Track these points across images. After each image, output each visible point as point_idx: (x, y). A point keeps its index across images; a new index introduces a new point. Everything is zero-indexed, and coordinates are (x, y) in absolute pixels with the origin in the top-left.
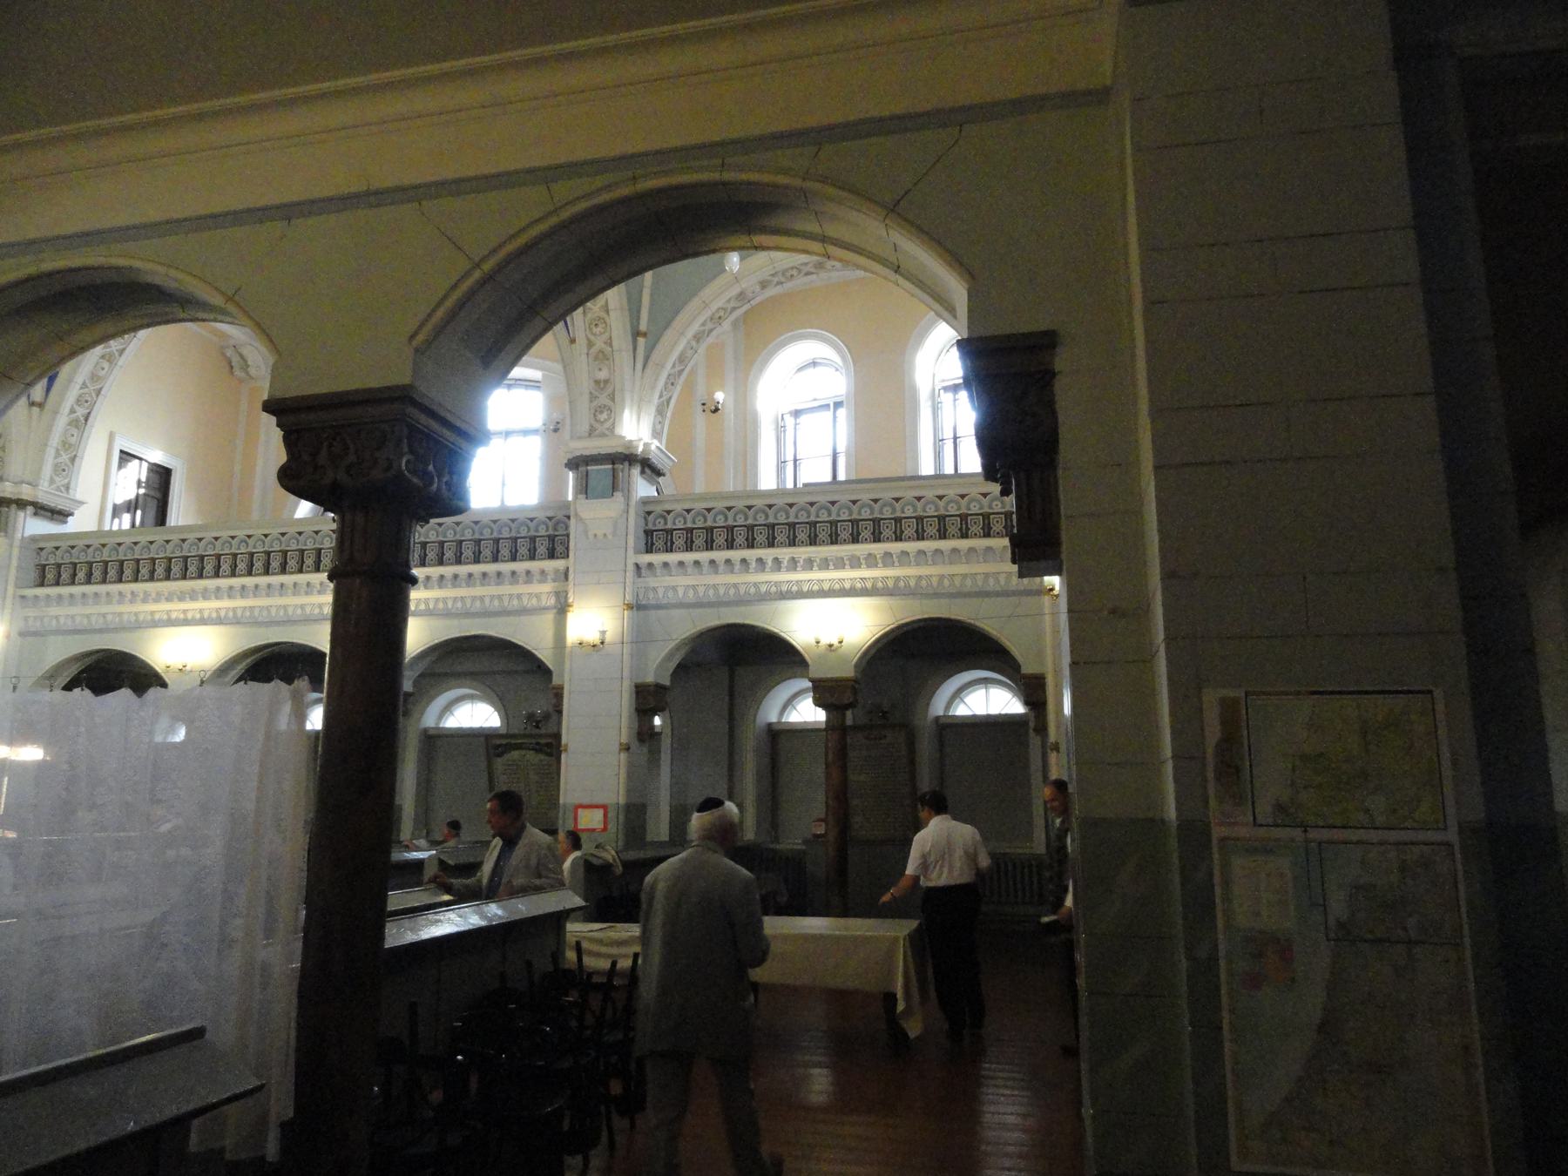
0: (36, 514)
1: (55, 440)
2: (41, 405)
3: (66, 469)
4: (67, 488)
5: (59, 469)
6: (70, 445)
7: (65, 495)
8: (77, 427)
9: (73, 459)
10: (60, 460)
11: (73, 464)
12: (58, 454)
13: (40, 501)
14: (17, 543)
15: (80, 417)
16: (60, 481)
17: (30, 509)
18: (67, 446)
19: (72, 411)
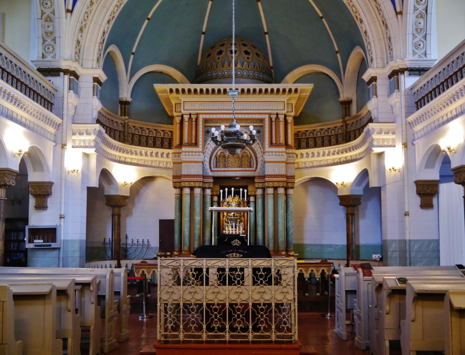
0: (410, 75)
1: (410, 29)
2: (401, 13)
3: (421, 43)
4: (425, 54)
5: (417, 46)
6: (421, 30)
7: (425, 58)
8: (421, 17)
9: (425, 37)
10: (417, 39)
11: (426, 40)
12: (414, 37)
13: (409, 67)
14: (403, 94)
15: (423, 11)
16: (419, 52)
17: (406, 73)
18: (419, 31)
19: (415, 9)
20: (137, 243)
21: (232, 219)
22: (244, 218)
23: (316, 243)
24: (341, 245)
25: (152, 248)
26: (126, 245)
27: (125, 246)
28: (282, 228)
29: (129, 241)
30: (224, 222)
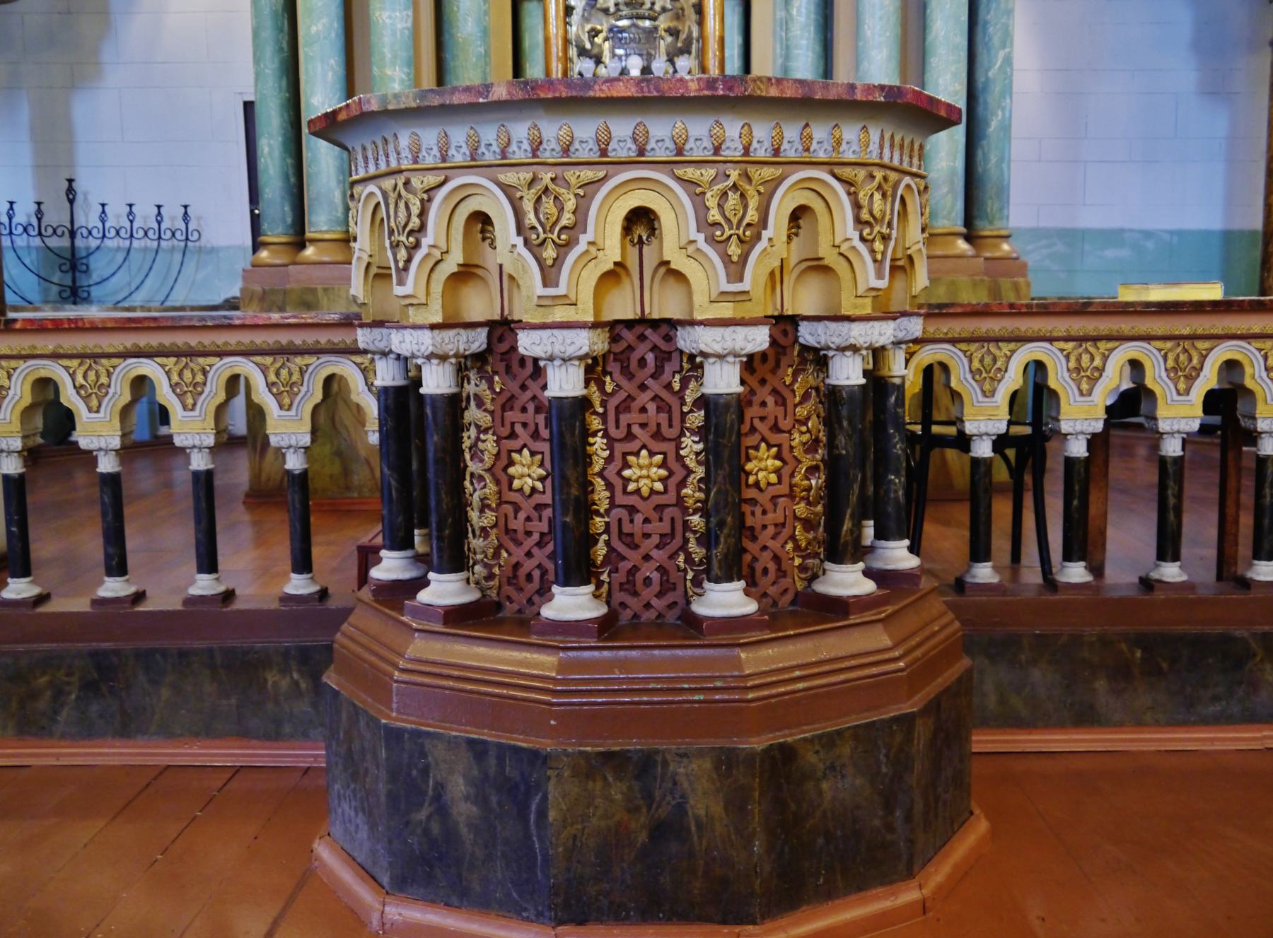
20: (128, 225)
21: (622, 30)
22: (701, 23)
23: (1042, 224)
24: (1172, 233)
25: (213, 250)
26: (73, 234)
27: (65, 242)
28: (958, 87)
29: (88, 218)
30: (573, 52)
